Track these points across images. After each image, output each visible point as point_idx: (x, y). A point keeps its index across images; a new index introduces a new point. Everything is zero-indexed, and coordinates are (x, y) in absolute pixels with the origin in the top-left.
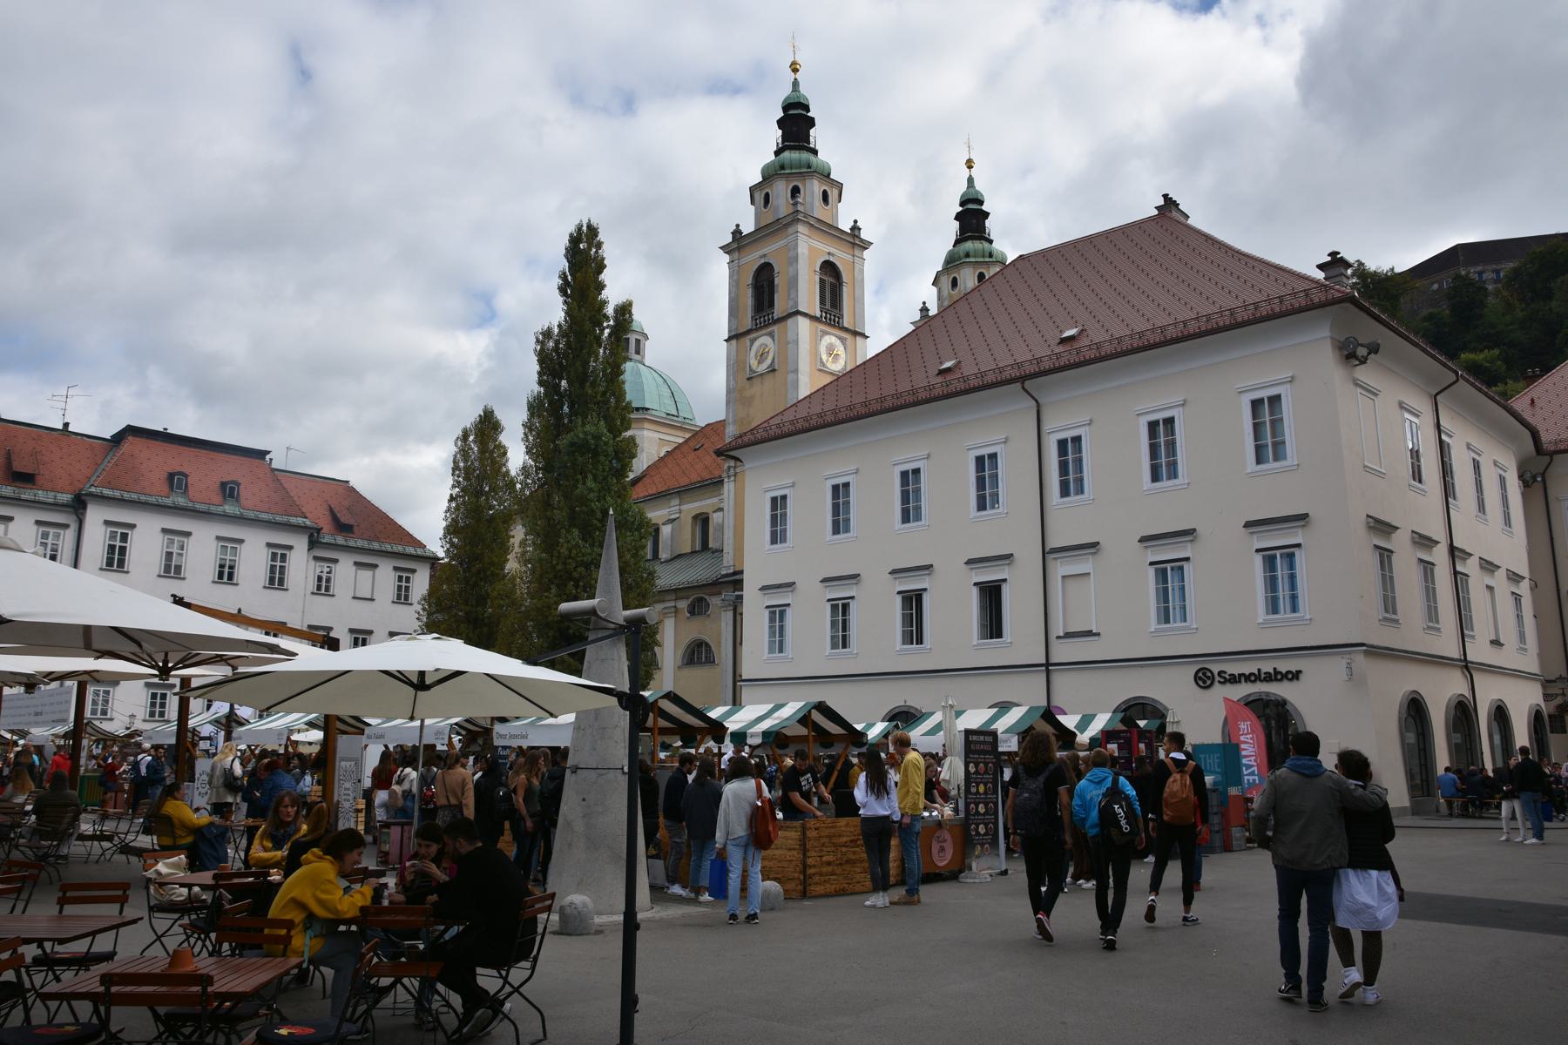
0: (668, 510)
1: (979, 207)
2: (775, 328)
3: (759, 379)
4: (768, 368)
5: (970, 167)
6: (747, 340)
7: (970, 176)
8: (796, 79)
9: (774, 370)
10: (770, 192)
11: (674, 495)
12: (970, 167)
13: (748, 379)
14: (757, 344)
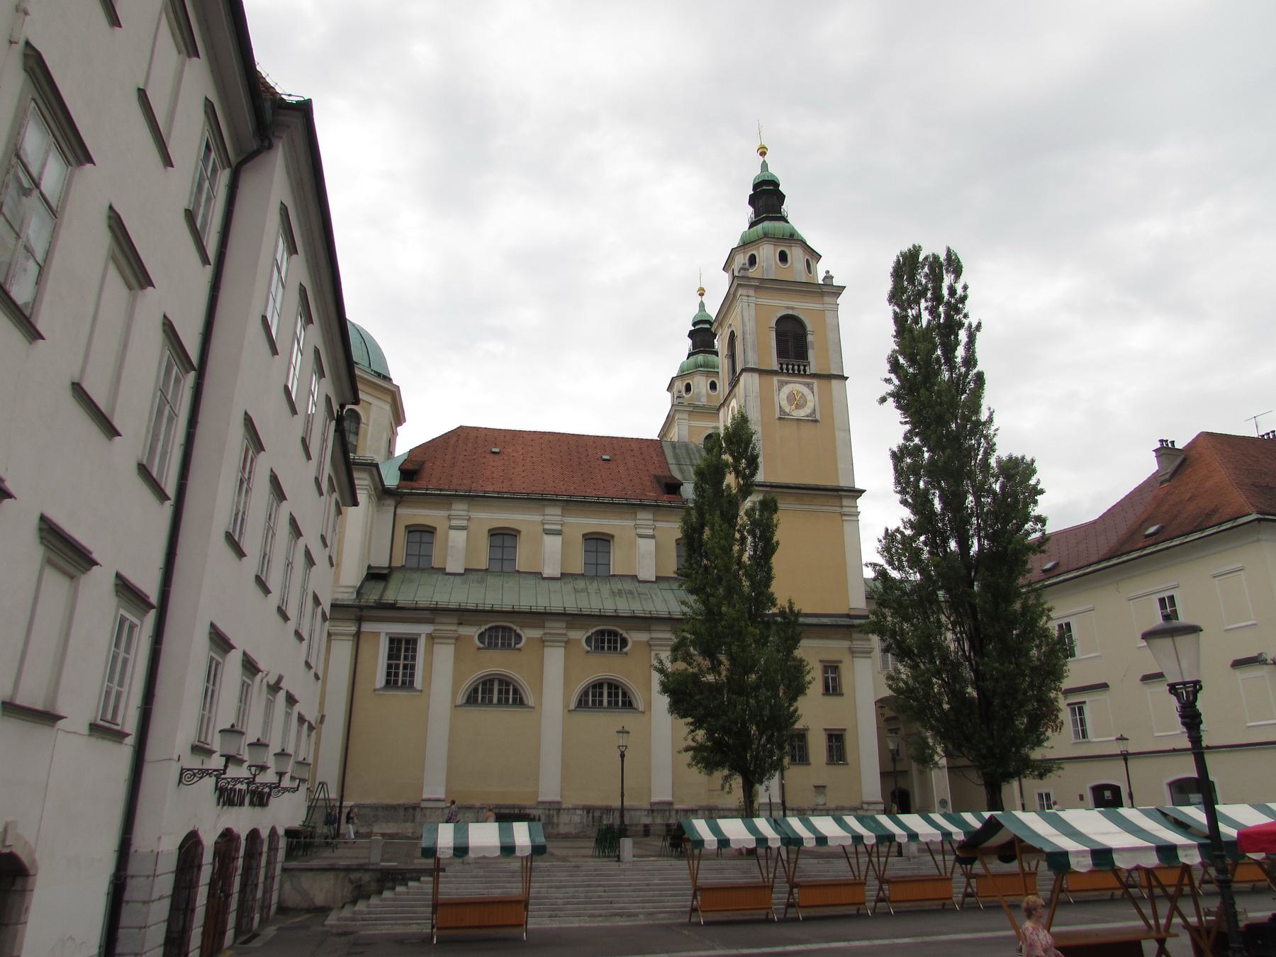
0: (542, 518)
1: (708, 326)
2: (815, 382)
3: (795, 423)
4: (807, 416)
5: (701, 295)
6: (775, 379)
7: (702, 302)
8: (764, 161)
9: (816, 421)
10: (788, 252)
11: (558, 503)
12: (701, 295)
13: (780, 419)
14: (786, 390)
